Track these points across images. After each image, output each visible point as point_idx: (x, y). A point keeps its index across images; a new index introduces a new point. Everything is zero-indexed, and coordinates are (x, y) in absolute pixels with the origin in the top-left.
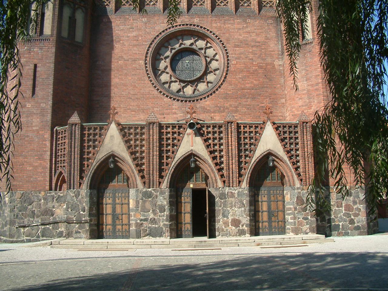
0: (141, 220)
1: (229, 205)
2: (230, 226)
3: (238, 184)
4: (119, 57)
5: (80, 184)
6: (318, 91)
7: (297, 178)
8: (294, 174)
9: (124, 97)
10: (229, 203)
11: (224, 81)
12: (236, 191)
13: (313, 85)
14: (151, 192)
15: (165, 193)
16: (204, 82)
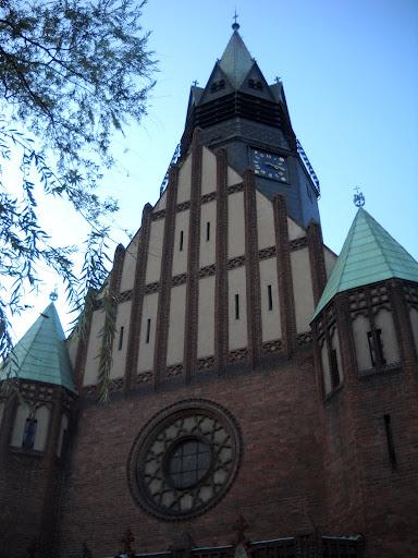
11: (234, 479)
16: (208, 485)
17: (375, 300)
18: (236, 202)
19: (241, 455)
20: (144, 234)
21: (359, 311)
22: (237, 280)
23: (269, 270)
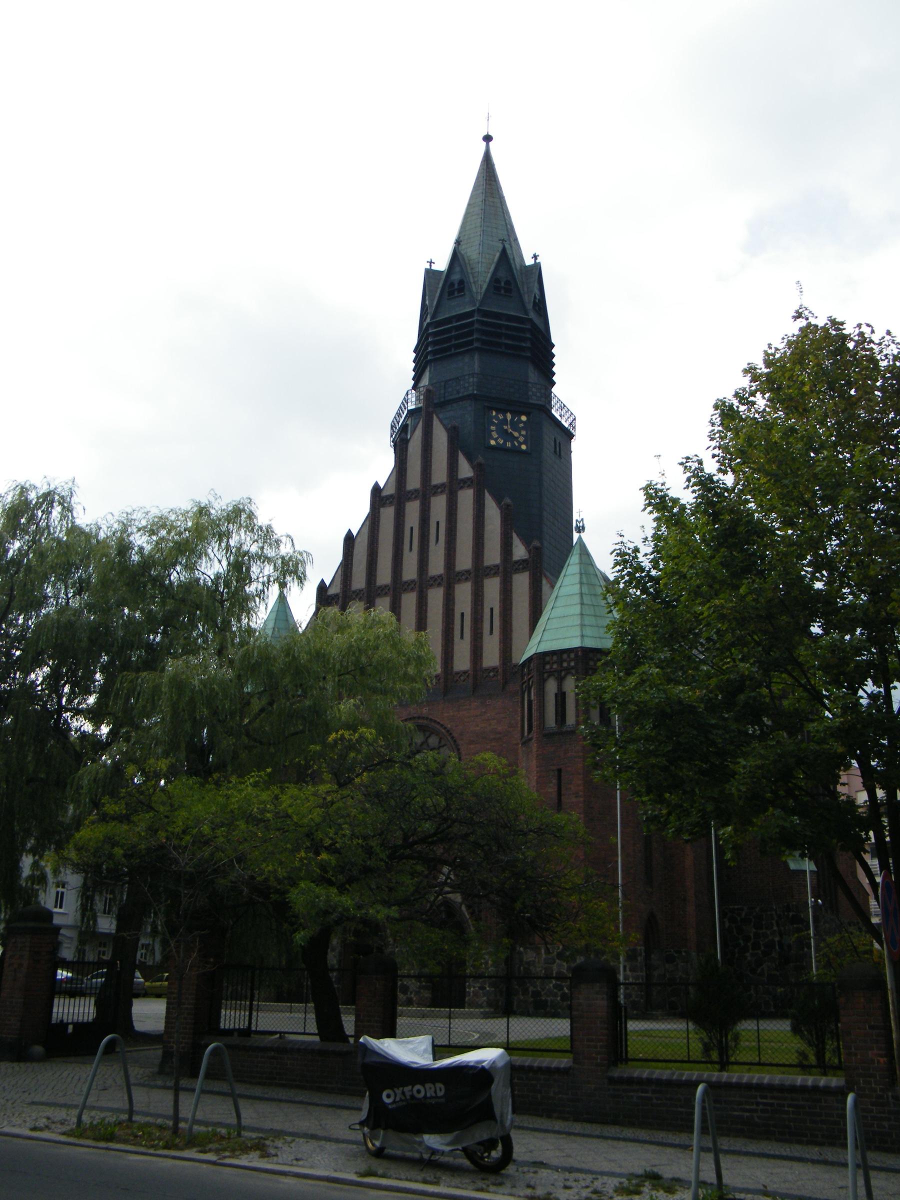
17: (565, 664)
18: (466, 497)
20: (373, 520)
21: (551, 673)
22: (464, 592)
23: (492, 587)
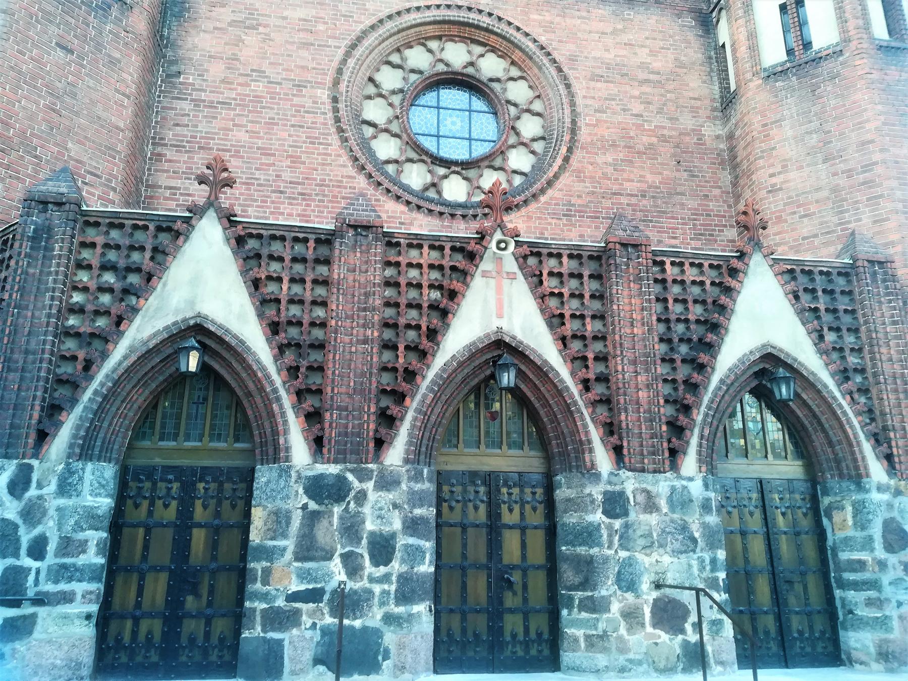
0: (294, 597)
1: (642, 542)
2: (649, 629)
3: (667, 463)
4: (252, 70)
5: (43, 436)
6: (870, 187)
7: (874, 449)
8: (862, 437)
9: (259, 185)
10: (639, 533)
12: (662, 485)
13: (849, 170)
14: (340, 479)
15: (398, 483)
19: (573, 131)
